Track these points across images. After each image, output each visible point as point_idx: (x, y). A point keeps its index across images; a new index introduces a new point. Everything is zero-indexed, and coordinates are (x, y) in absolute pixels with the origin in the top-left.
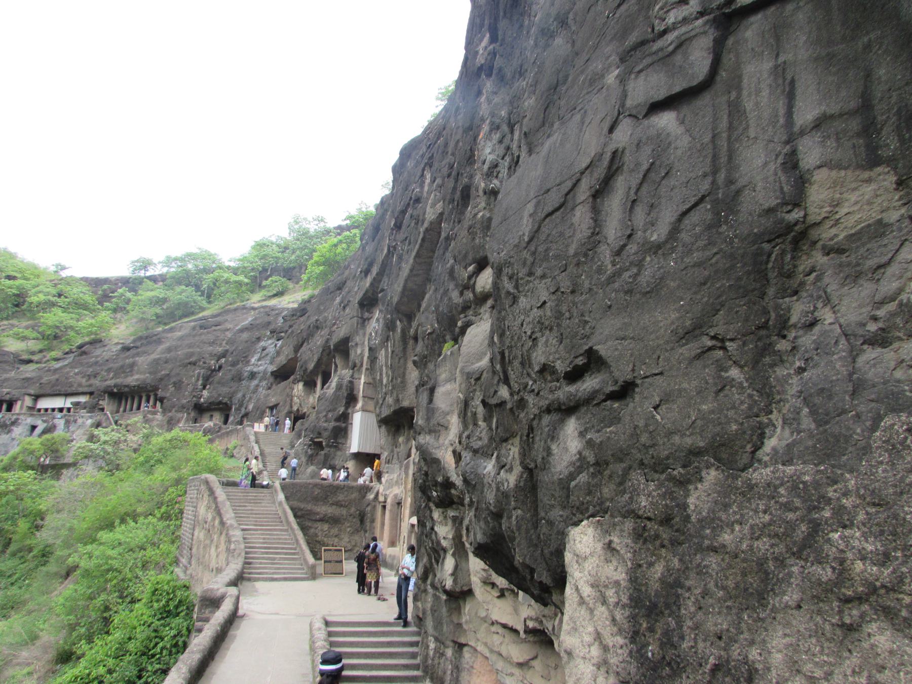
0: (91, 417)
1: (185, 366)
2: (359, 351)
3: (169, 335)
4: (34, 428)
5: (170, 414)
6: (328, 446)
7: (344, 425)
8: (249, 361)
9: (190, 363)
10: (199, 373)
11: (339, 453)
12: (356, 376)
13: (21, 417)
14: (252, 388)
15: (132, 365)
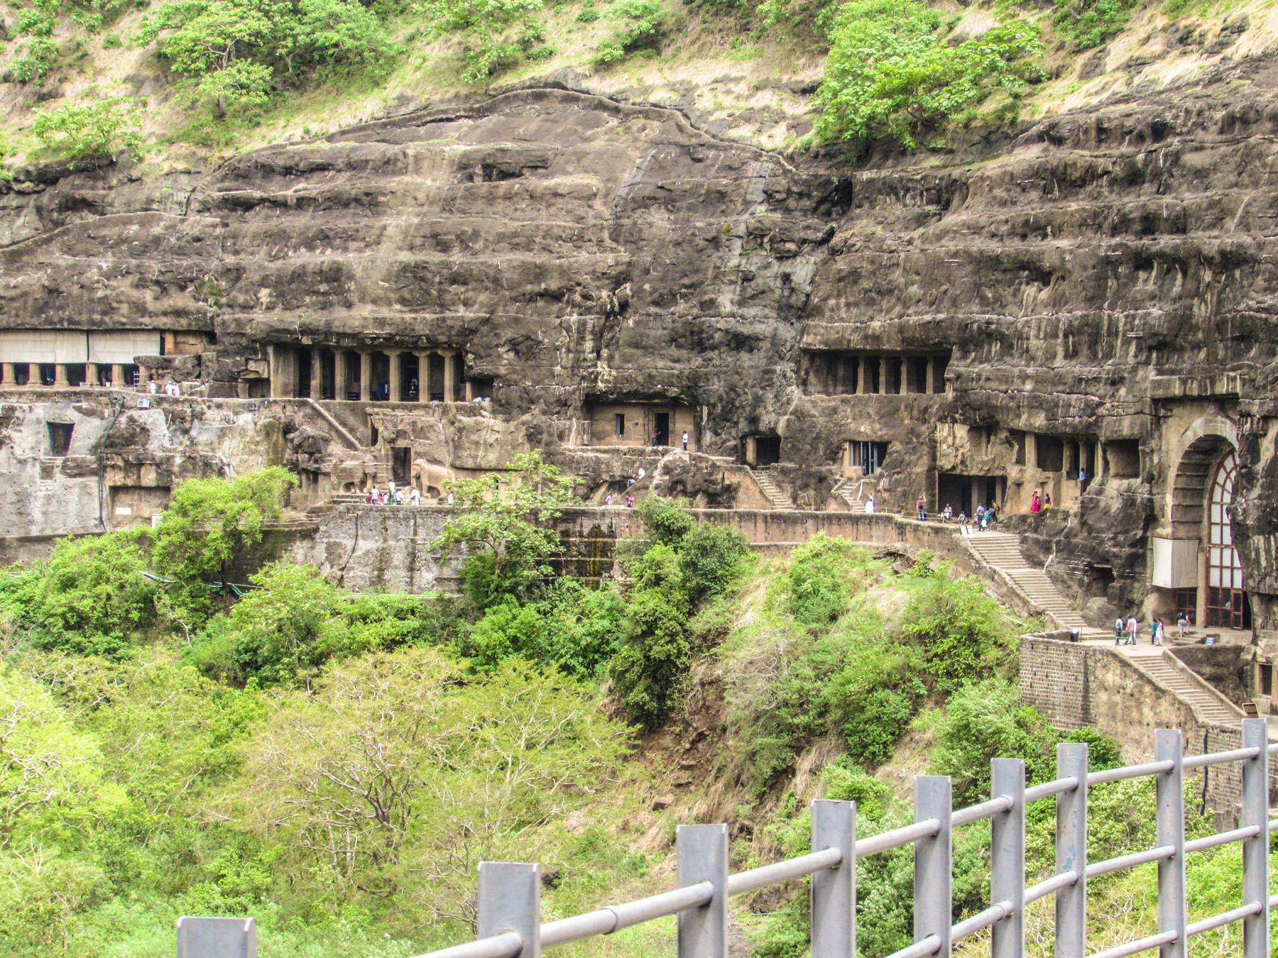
0: (250, 408)
1: (531, 298)
2: (1156, 460)
3: (393, 183)
4: (60, 434)
5: (526, 417)
6: (1122, 576)
7: (1141, 551)
8: (712, 303)
9: (544, 295)
10: (583, 325)
11: (1136, 585)
12: (1155, 491)
13: (13, 401)
14: (750, 376)
15: (335, 275)
